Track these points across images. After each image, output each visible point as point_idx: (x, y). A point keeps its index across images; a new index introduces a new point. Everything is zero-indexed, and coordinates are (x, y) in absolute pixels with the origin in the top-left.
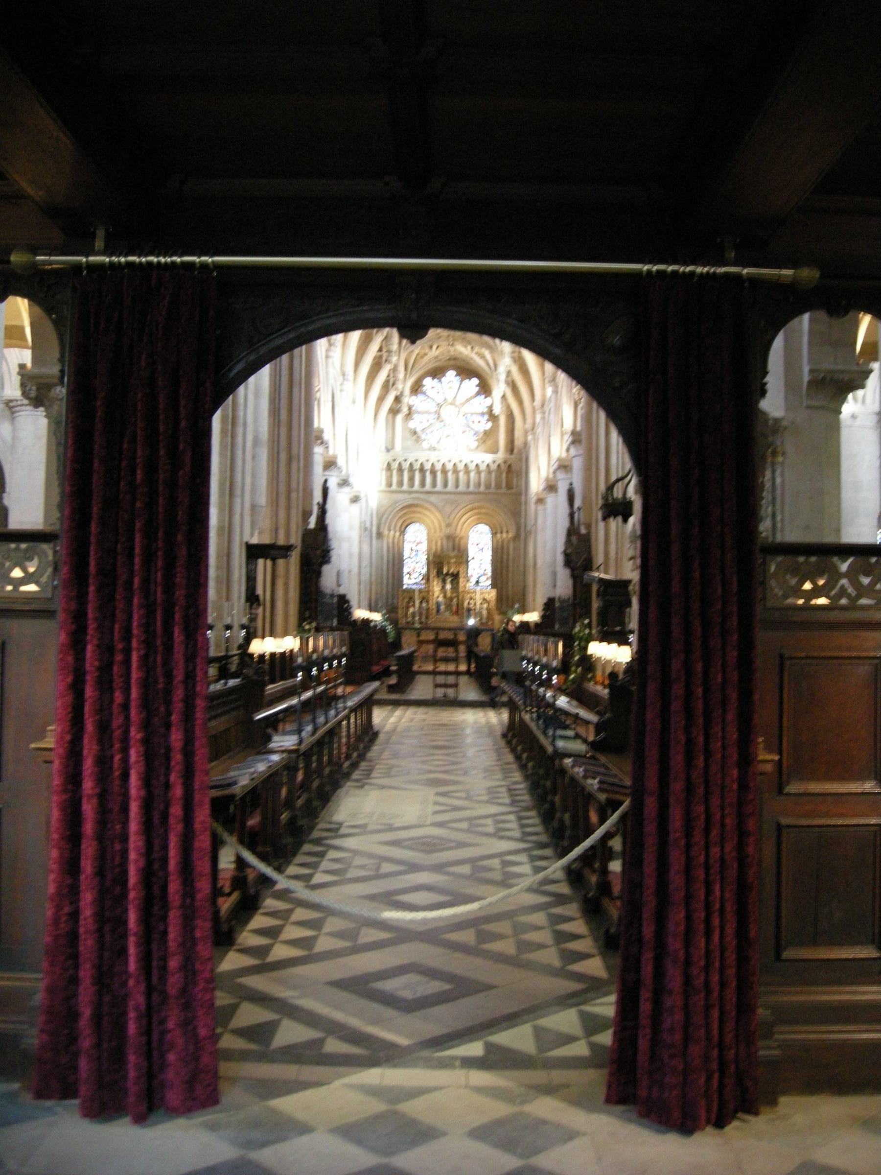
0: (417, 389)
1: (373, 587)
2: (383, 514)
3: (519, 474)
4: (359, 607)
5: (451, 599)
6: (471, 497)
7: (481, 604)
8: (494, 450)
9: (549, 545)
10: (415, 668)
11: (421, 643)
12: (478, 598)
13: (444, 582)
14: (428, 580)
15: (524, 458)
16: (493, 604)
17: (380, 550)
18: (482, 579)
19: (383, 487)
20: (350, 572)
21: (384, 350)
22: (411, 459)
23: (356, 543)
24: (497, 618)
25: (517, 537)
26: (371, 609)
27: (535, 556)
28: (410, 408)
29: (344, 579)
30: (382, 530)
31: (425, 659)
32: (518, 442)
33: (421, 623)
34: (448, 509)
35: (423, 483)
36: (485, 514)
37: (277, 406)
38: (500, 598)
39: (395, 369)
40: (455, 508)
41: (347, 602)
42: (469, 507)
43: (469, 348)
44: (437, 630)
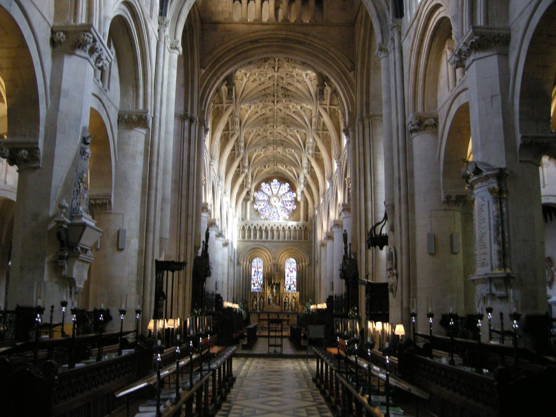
0: (258, 188)
1: (235, 291)
3: (311, 232)
4: (228, 301)
5: (276, 297)
6: (286, 244)
8: (298, 220)
9: (328, 268)
10: (257, 334)
11: (260, 320)
12: (290, 297)
13: (272, 288)
14: (264, 287)
15: (313, 224)
16: (298, 299)
17: (239, 272)
18: (292, 286)
19: (241, 239)
20: (222, 282)
21: (241, 167)
22: (255, 224)
23: (226, 267)
24: (300, 307)
25: (310, 265)
26: (234, 302)
27: (320, 274)
28: (254, 199)
30: (240, 260)
31: (263, 328)
33: (260, 309)
34: (274, 250)
35: (261, 237)
36: (294, 253)
38: (301, 296)
39: (246, 177)
41: (221, 298)
42: (286, 249)
43: (285, 167)
44: (268, 314)
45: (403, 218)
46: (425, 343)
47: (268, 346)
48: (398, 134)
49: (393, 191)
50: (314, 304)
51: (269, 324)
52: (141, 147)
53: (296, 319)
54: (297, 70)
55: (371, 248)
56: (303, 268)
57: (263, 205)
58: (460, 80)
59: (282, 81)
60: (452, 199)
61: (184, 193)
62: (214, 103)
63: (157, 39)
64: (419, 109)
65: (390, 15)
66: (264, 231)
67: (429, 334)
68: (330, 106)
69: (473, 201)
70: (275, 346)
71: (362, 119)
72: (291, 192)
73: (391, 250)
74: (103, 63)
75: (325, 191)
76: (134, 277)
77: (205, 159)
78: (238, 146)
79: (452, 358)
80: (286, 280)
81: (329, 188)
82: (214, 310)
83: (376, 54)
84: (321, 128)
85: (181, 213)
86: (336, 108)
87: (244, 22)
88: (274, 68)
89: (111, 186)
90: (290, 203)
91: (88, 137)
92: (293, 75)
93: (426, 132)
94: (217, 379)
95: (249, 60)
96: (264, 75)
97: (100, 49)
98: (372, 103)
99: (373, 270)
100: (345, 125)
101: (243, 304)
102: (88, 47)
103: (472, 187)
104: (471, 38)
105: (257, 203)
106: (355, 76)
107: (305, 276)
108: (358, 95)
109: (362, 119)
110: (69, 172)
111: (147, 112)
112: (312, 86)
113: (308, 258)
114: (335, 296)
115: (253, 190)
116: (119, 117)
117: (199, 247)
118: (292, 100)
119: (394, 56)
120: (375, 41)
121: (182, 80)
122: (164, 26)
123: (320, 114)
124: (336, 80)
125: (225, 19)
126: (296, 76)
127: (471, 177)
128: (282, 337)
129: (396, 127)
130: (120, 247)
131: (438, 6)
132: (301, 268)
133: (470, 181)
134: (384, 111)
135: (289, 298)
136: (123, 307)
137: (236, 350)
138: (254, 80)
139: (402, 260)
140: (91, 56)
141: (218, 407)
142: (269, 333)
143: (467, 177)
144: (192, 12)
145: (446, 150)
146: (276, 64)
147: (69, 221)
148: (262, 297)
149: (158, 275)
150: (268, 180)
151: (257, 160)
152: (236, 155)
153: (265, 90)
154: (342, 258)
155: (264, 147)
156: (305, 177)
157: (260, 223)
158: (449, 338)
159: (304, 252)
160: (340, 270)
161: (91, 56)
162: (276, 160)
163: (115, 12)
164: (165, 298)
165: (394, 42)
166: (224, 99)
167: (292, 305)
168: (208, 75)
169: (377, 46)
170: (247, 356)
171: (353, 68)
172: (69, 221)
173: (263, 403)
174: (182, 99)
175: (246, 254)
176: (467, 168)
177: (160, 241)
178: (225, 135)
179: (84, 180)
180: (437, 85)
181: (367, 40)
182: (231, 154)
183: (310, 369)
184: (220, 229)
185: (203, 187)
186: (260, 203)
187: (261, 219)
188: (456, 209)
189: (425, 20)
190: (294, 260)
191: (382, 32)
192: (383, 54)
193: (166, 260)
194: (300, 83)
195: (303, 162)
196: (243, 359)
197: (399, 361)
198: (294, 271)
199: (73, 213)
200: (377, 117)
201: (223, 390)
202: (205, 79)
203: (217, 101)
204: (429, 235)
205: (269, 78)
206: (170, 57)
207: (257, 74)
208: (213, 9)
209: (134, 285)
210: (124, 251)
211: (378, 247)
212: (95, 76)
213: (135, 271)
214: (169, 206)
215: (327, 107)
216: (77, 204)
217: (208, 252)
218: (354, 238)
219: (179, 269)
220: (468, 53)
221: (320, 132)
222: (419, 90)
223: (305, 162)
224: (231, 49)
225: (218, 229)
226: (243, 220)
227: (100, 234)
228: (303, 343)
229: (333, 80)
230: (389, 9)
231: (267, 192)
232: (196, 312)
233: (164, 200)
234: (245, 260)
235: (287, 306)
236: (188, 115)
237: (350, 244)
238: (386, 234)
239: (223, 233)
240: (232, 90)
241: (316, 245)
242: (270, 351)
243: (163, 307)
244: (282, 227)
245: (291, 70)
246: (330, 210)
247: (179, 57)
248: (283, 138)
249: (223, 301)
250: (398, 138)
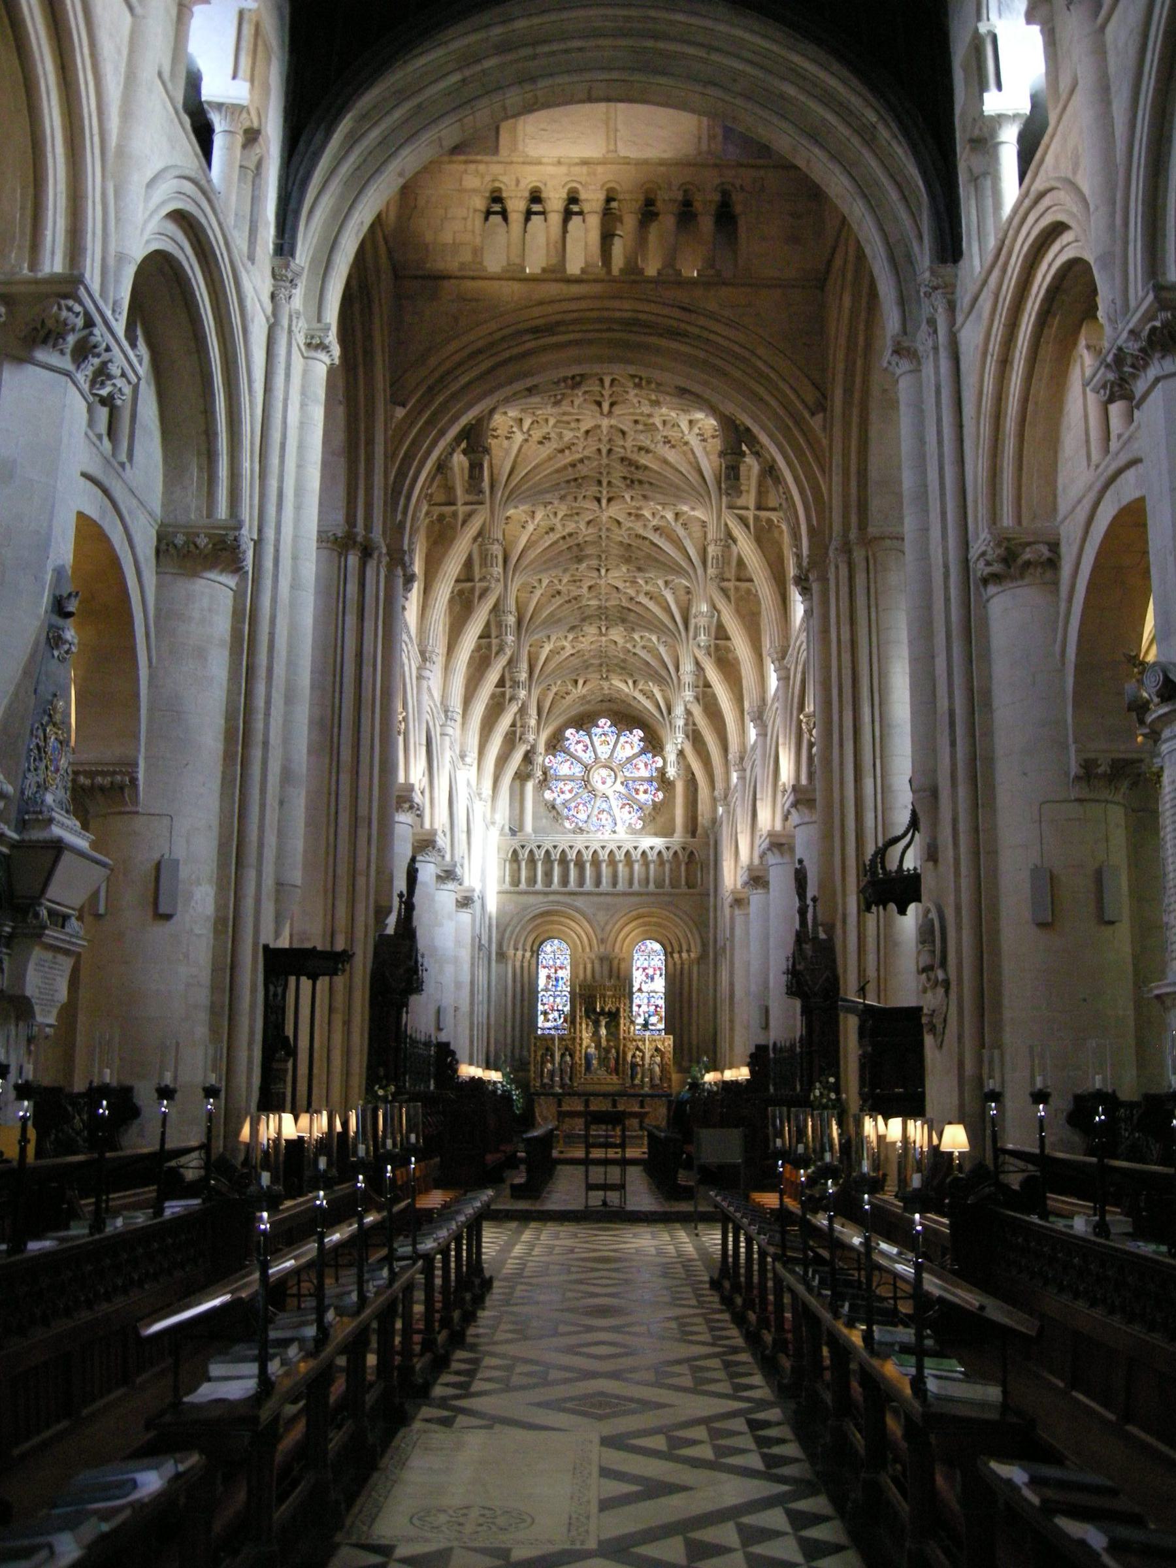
0: (556, 744)
2: (508, 925)
3: (704, 866)
4: (471, 1064)
5: (607, 1051)
7: (652, 1056)
8: (667, 832)
9: (755, 967)
10: (555, 1154)
11: (562, 1115)
12: (648, 1048)
13: (597, 1024)
14: (573, 1022)
15: (712, 842)
16: (669, 1055)
17: (502, 978)
18: (653, 1020)
19: (507, 886)
20: (456, 1009)
21: (508, 684)
22: (548, 845)
23: (466, 967)
24: (675, 1077)
25: (703, 957)
26: (488, 1067)
27: (732, 984)
28: (545, 773)
29: (448, 1020)
30: (505, 949)
31: (570, 1139)
32: (703, 819)
33: (562, 1086)
34: (601, 917)
35: (565, 881)
37: (335, 740)
38: (678, 1047)
39: (523, 710)
40: (612, 916)
41: (453, 1053)
42: (634, 913)
43: (630, 683)
44: (587, 1096)
45: (963, 826)
46: (1026, 1174)
47: (584, 1186)
48: (946, 588)
49: (934, 751)
50: (715, 1069)
51: (587, 1128)
52: (222, 625)
53: (663, 1111)
54: (664, 410)
55: (874, 909)
56: (682, 964)
58: (1119, 436)
59: (621, 443)
60: (1100, 770)
61: (346, 754)
62: (430, 505)
63: (268, 319)
64: (1007, 519)
65: (924, 256)
66: (572, 865)
67: (1037, 1151)
68: (757, 513)
69: (1159, 775)
70: (605, 1187)
71: (846, 549)
72: (650, 755)
73: (930, 916)
74: (114, 385)
75: (745, 752)
76: (202, 996)
77: (406, 661)
78: (499, 625)
79: (1103, 1217)
80: (636, 1001)
81: (756, 742)
82: (432, 1088)
83: (885, 365)
84: (731, 573)
85: (337, 813)
86: (774, 516)
87: (515, 274)
88: (599, 404)
89: (136, 736)
90: (646, 786)
91: (70, 595)
92: (654, 424)
93: (1026, 581)
94: (438, 1282)
95: (529, 382)
96: (573, 425)
97: (104, 345)
98: (876, 504)
99: (878, 970)
100: (799, 565)
101: (514, 1070)
102: (71, 339)
103: (1155, 736)
104: (1149, 316)
105: (553, 784)
106: (827, 427)
107: (690, 992)
108: (837, 479)
109: (846, 549)
110: (16, 694)
111: (239, 527)
112: (707, 454)
113: (698, 941)
114: (775, 1044)
115: (541, 748)
116: (159, 539)
117: (390, 911)
118: (649, 494)
119: (934, 370)
120: (883, 328)
121: (340, 437)
122: (288, 284)
123: (730, 535)
124: (771, 436)
125: (463, 266)
126: (661, 428)
127: (1152, 706)
128: (624, 1163)
129: (942, 570)
130: (163, 909)
131: (1058, 229)
132: (678, 967)
133: (1149, 719)
134: (909, 526)
135: (644, 1053)
136: (168, 1079)
137: (492, 1200)
138: (545, 438)
139: (960, 943)
140: (78, 367)
141: (441, 1363)
142: (588, 1153)
143: (1140, 708)
144: (368, 246)
145: (1081, 634)
146: (606, 393)
147: (15, 836)
148: (569, 1051)
149: (272, 988)
150: (584, 722)
151: (552, 665)
152: (494, 649)
153: (573, 465)
154: (791, 939)
155: (572, 628)
156: (688, 713)
157: (563, 841)
158: (1094, 1160)
159: (686, 923)
160: (787, 972)
161: (78, 367)
162: (607, 664)
163: (148, 242)
164: (292, 1052)
165: (935, 331)
166: (459, 492)
167: (651, 1071)
168: (412, 424)
169: (889, 343)
170: (525, 1218)
171: (821, 406)
172: (15, 836)
173: (571, 1350)
174: (341, 491)
175: (523, 928)
176: (1140, 682)
177: (278, 891)
178: (461, 593)
179: (58, 718)
180: (1056, 452)
181: (862, 327)
182: (478, 648)
183: (702, 1251)
184: (448, 857)
185: (401, 739)
187: (565, 832)
188: (1110, 798)
189: (1022, 267)
190: (657, 946)
191: (902, 302)
192: (905, 365)
193: (295, 946)
194: (673, 447)
195: (681, 668)
196: (514, 1225)
197: (951, 1226)
198: (656, 977)
199: (27, 813)
200: (888, 542)
201: (456, 1315)
202: (405, 434)
203: (440, 497)
204: (1036, 871)
205: (587, 432)
206: (305, 372)
207: (552, 421)
208: (429, 237)
209: (203, 1016)
210: (175, 918)
211: (892, 907)
212: (91, 423)
213: (205, 976)
214: (303, 793)
215: (750, 515)
216: (39, 786)
217: (415, 923)
218: (826, 883)
219: (333, 973)
220: (1142, 361)
221: (730, 585)
222: (1005, 465)
223: (687, 667)
224: (480, 351)
225: (443, 857)
226: (513, 832)
227: (104, 872)
228: (684, 1178)
229: (764, 438)
230: (921, 237)
232: (381, 1093)
233: (287, 776)
234: (520, 946)
235: (639, 1076)
236: (356, 534)
237: (814, 900)
238: (915, 869)
239: (458, 871)
240: (481, 466)
241: (719, 898)
242: (591, 1203)
243: (285, 1082)
244: (624, 851)
245: (646, 409)
246: (758, 803)
247: (331, 371)
248: (625, 604)
249: (457, 1062)
250: (947, 600)
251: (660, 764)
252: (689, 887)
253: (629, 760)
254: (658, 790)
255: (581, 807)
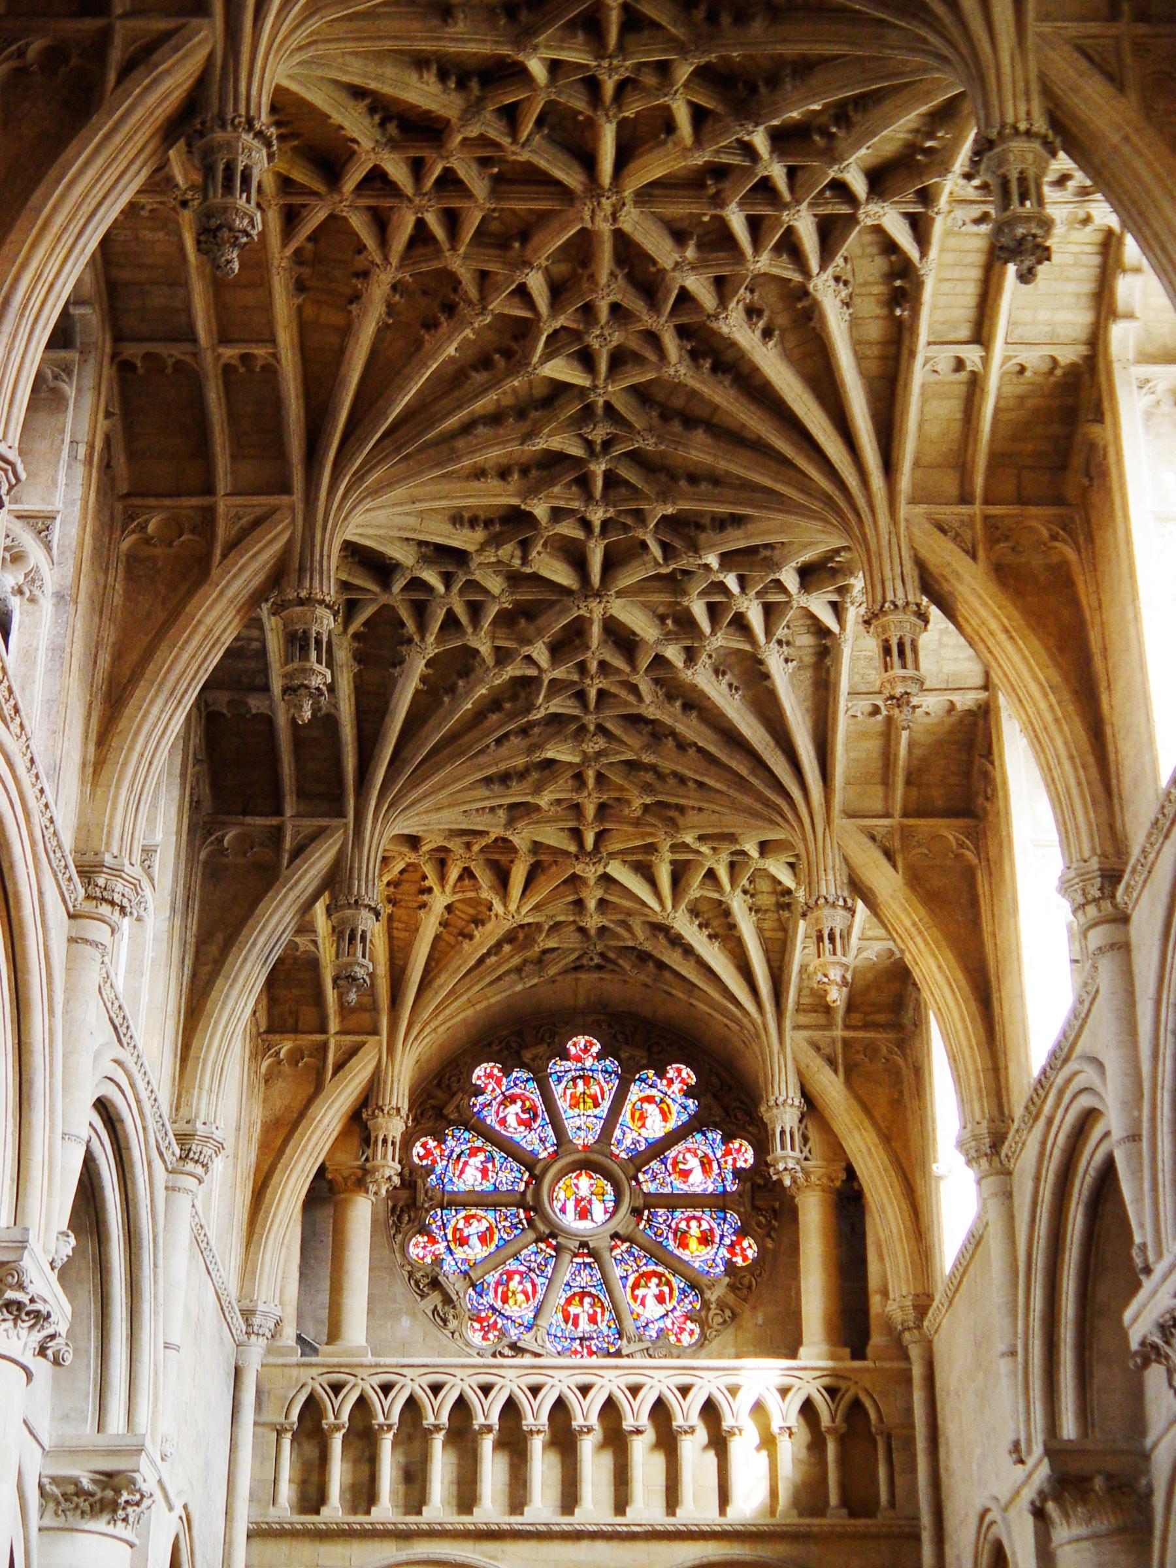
57: (484, 1239)
186: (456, 1219)
231: (515, 1132)
251: (746, 1157)
252: (852, 1514)
253: (658, 1149)
254: (742, 1233)
255: (514, 1284)
